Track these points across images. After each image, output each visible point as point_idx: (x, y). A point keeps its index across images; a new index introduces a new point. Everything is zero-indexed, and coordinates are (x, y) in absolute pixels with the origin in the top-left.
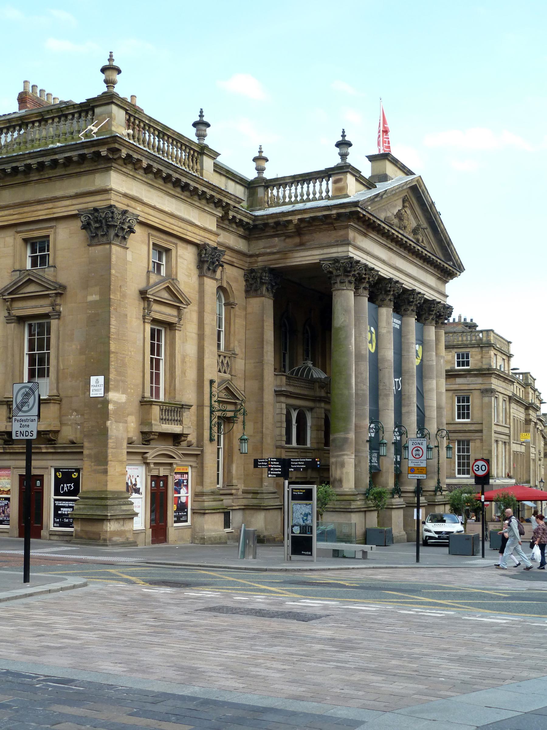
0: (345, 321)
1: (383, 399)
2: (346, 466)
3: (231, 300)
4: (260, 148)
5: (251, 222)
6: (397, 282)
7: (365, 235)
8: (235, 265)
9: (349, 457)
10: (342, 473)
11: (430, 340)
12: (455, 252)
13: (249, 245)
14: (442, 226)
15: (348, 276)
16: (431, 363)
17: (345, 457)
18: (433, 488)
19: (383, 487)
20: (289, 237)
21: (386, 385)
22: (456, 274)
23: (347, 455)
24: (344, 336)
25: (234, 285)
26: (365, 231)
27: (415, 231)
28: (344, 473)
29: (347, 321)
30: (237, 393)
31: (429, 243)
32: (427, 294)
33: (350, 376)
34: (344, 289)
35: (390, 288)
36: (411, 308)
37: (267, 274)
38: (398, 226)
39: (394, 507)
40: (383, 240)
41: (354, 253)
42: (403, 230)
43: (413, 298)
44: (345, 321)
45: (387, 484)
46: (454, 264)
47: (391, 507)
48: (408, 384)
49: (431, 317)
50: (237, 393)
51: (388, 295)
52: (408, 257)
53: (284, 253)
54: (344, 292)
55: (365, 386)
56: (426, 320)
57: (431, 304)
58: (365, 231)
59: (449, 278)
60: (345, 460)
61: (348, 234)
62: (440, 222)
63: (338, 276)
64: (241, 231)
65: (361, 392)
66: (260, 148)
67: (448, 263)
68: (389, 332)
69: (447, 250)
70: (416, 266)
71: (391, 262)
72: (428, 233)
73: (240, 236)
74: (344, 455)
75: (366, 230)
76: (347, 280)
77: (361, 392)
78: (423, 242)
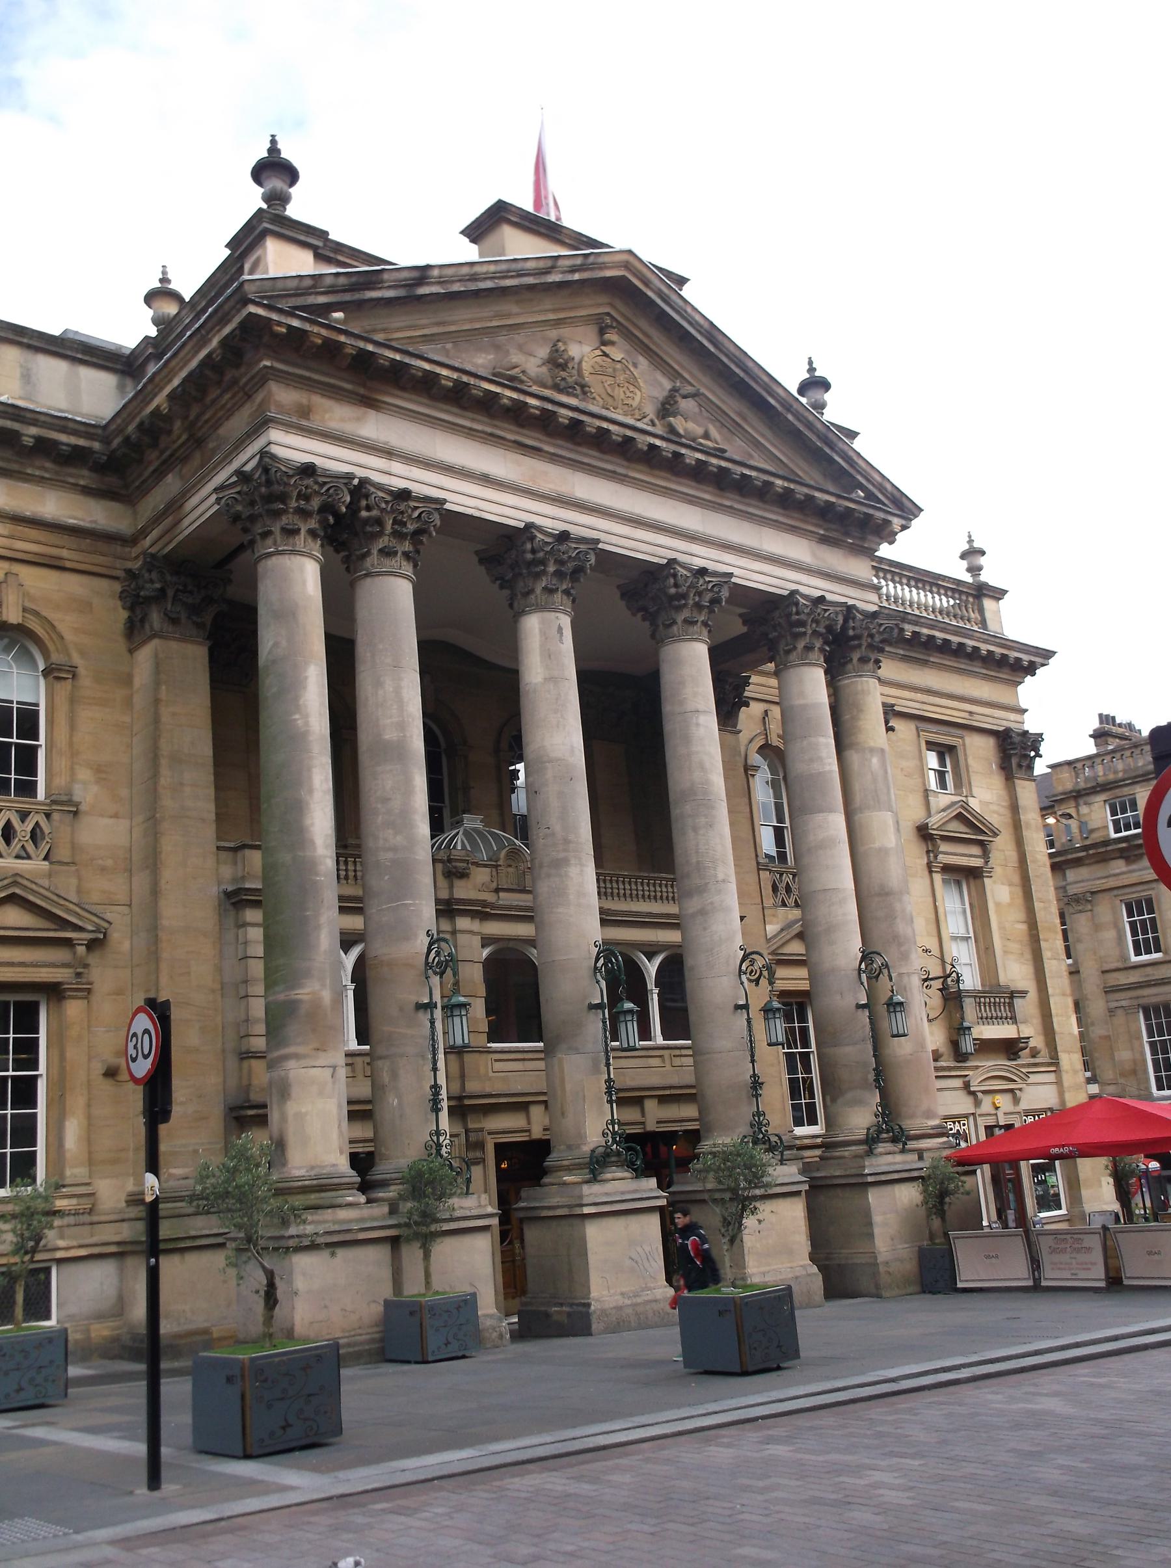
0: (276, 644)
1: (549, 876)
2: (295, 1091)
3: (55, 658)
4: (164, 273)
5: (96, 445)
6: (564, 536)
7: (369, 403)
8: (68, 564)
9: (304, 1063)
10: (284, 1119)
11: (804, 707)
12: (860, 462)
13: (135, 513)
14: (780, 391)
15: (277, 514)
16: (816, 767)
17: (291, 1064)
18: (861, 1134)
19: (569, 1147)
20: (185, 459)
21: (553, 834)
22: (887, 523)
23: (297, 1056)
24: (274, 690)
25: (66, 623)
26: (362, 391)
27: (666, 409)
28: (290, 1118)
29: (284, 643)
30: (69, 911)
31: (757, 445)
32: (736, 571)
33: (298, 808)
34: (270, 555)
35: (533, 551)
36: (680, 618)
37: (154, 575)
38: (550, 382)
39: (586, 1210)
40: (473, 420)
41: (291, 447)
42: (576, 396)
43: (676, 585)
44: (276, 644)
45: (581, 1136)
46: (870, 495)
47: (578, 1211)
48: (695, 829)
49: (801, 645)
50: (69, 911)
51: (538, 576)
52: (632, 474)
53: (175, 506)
54: (274, 560)
55: (399, 838)
56: (788, 652)
57: (788, 606)
58: (362, 391)
59: (878, 540)
60: (292, 1074)
61: (270, 393)
62: (765, 379)
63: (253, 519)
64: (85, 477)
65: (390, 855)
66: (164, 273)
67: (853, 496)
68: (551, 679)
69: (831, 461)
70: (691, 503)
71: (546, 487)
72: (745, 419)
73: (87, 491)
74: (286, 1057)
75: (364, 386)
76: (276, 529)
77: (390, 855)
78: (706, 436)
